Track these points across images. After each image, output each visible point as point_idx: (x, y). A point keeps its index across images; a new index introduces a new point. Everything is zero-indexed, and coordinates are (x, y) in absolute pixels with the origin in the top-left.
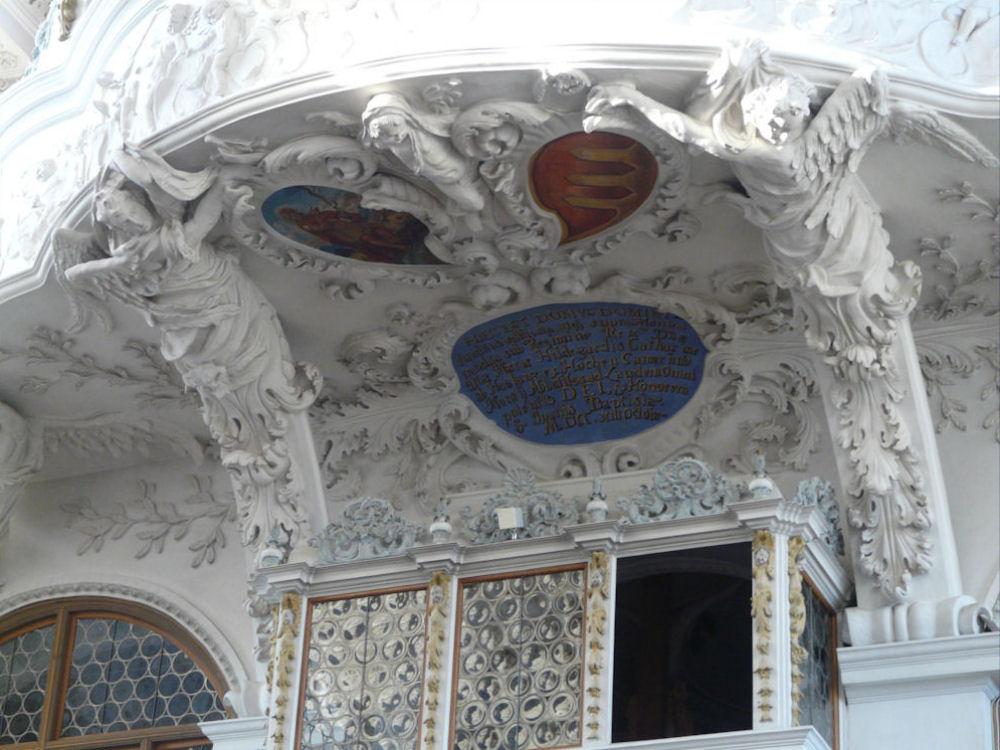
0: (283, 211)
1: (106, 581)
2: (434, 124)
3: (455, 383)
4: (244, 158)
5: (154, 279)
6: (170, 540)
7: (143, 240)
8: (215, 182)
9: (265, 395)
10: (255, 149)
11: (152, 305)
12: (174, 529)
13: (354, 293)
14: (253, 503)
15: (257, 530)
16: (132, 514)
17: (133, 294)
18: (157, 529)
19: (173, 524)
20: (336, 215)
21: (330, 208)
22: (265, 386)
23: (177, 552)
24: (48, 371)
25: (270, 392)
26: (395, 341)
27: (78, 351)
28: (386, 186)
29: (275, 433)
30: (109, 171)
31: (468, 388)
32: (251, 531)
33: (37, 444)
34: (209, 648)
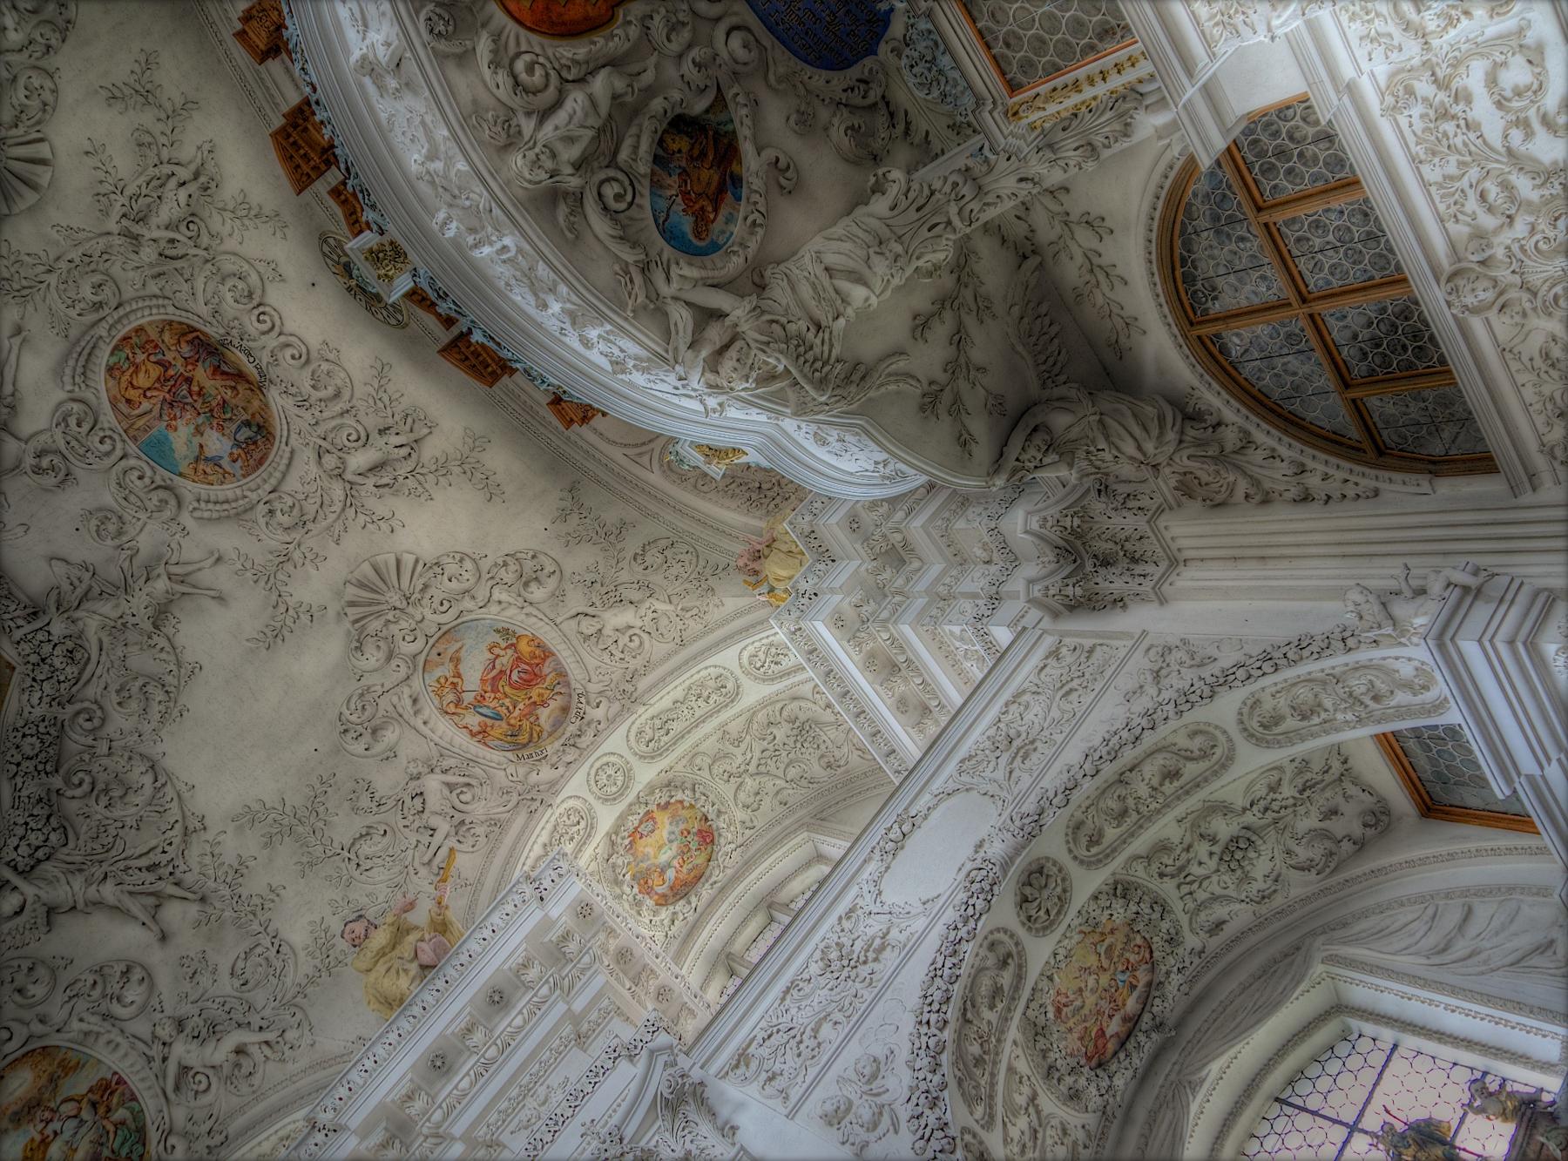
0: (698, 235)
1: (1153, 304)
2: (528, 126)
3: (868, 62)
4: (638, 279)
5: (792, 328)
6: (1104, 261)
7: (753, 345)
8: (675, 299)
9: (896, 212)
10: (627, 272)
11: (824, 324)
12: (1096, 260)
13: (782, 164)
14: (1003, 193)
15: (1021, 180)
16: (1100, 300)
17: (818, 341)
18: (1101, 277)
19: (1092, 264)
20: (685, 195)
21: (679, 200)
22: (888, 214)
23: (1110, 253)
24: (974, 399)
25: (892, 209)
26: (836, 121)
27: (943, 378)
28: (624, 155)
29: (926, 192)
30: (710, 386)
31: (872, 51)
32: (1023, 185)
33: (1057, 392)
34: (1163, 194)
